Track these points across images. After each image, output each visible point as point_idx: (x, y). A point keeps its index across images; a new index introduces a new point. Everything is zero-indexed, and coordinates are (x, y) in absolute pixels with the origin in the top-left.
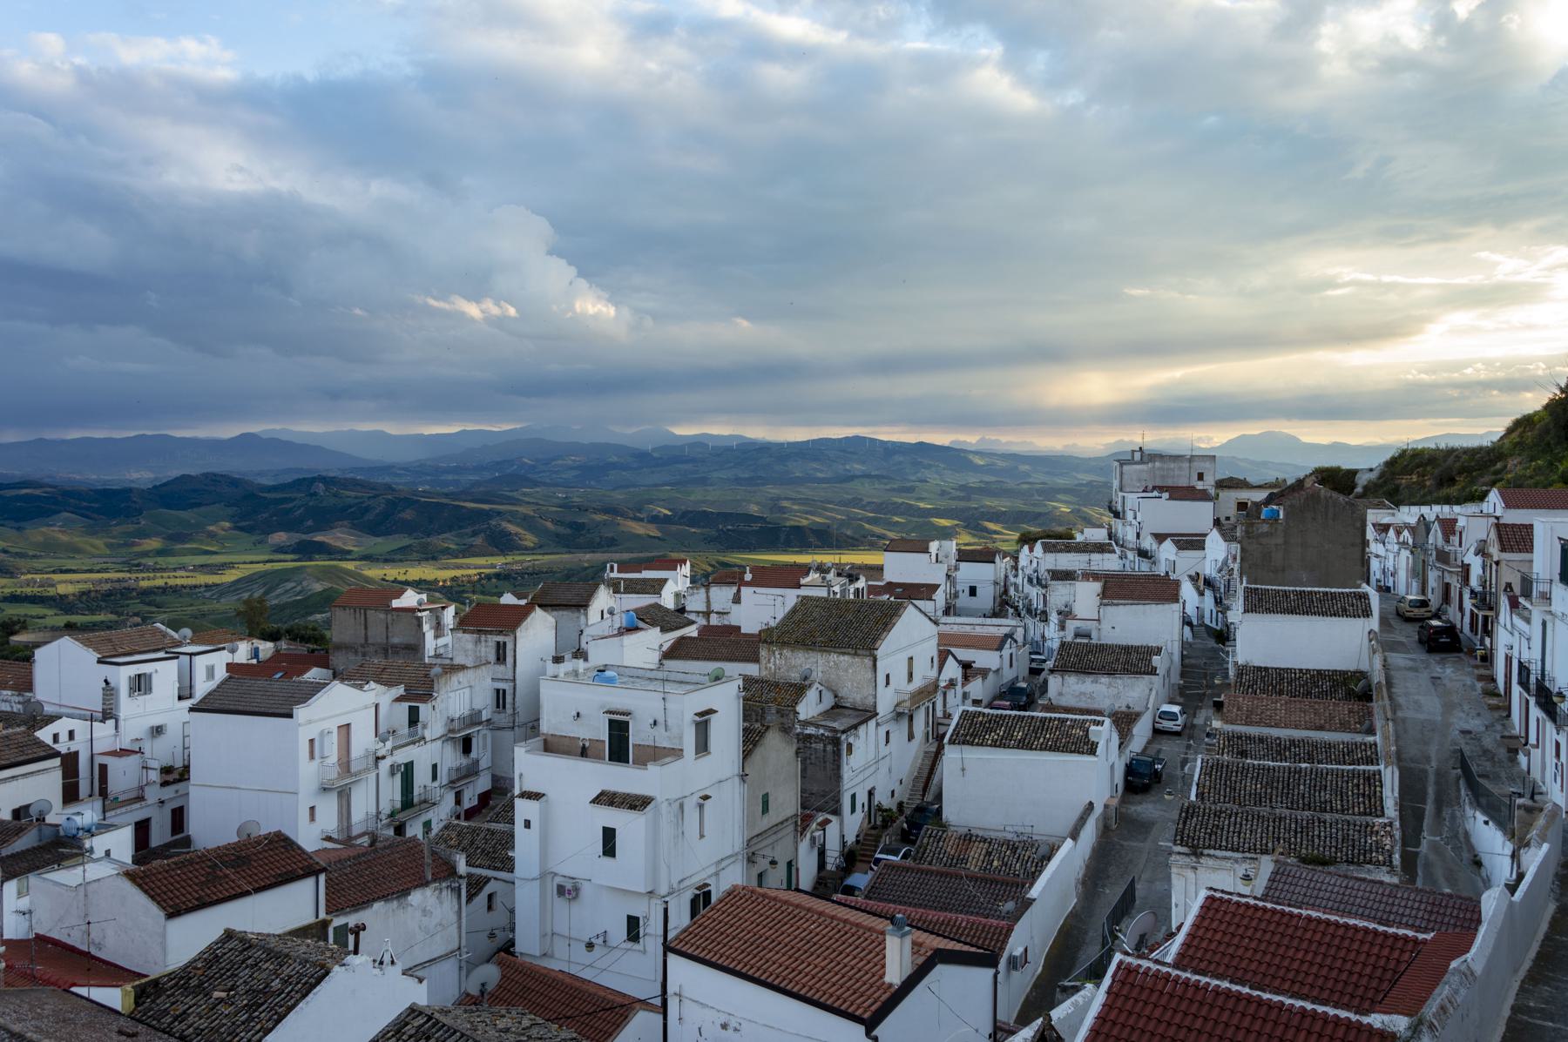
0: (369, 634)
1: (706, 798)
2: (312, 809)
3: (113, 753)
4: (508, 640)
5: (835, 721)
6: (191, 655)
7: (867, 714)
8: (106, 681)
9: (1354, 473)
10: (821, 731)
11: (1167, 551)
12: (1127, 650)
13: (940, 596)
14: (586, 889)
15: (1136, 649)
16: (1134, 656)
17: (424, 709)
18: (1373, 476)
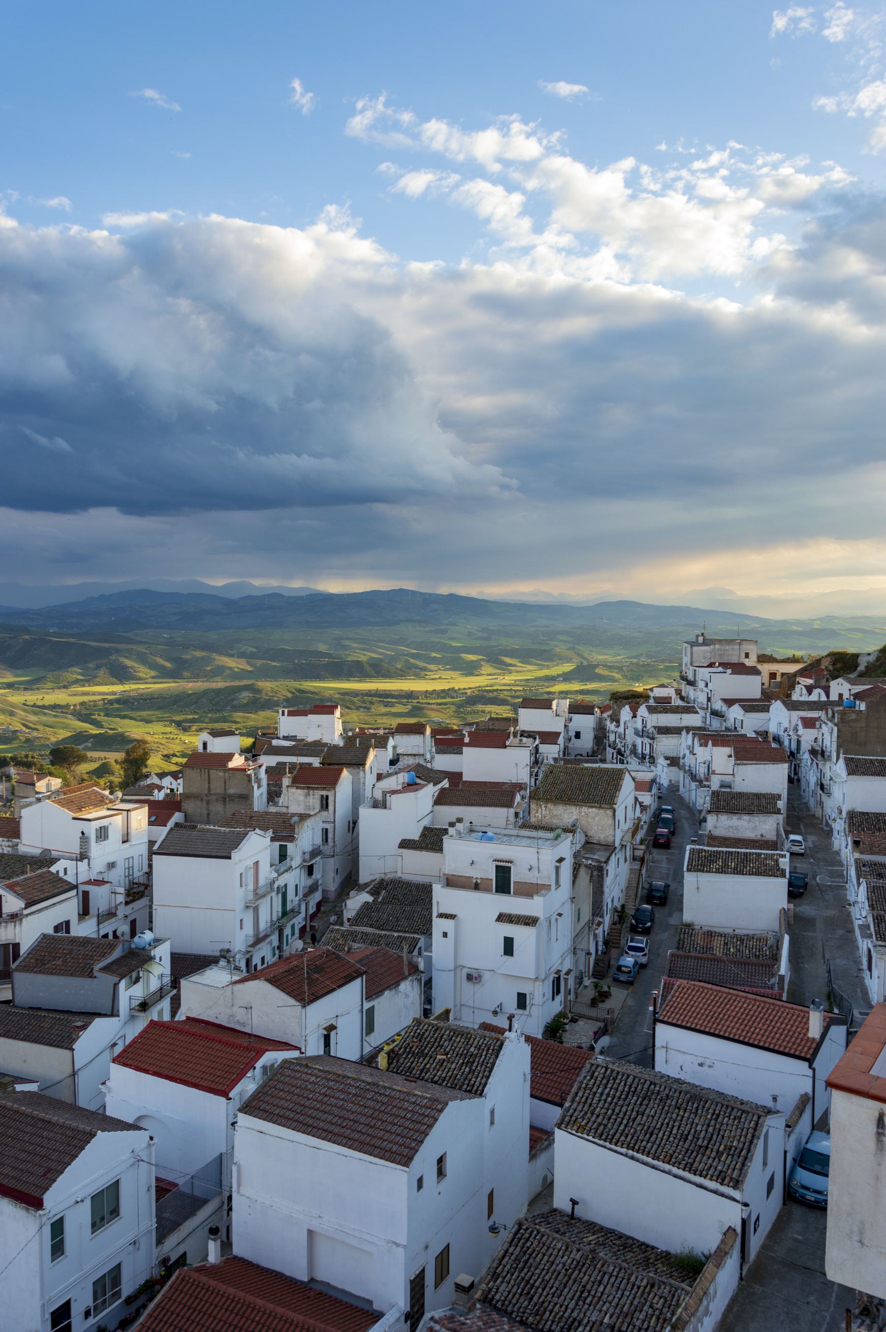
0: (212, 786)
1: (560, 915)
2: (241, 920)
3: (89, 882)
4: (330, 794)
5: (594, 854)
6: (128, 811)
7: (610, 848)
8: (83, 833)
9: (856, 656)
10: (590, 862)
11: (735, 713)
12: (758, 796)
13: (561, 740)
14: (487, 976)
15: (764, 796)
16: (763, 801)
17: (290, 846)
18: (871, 659)
